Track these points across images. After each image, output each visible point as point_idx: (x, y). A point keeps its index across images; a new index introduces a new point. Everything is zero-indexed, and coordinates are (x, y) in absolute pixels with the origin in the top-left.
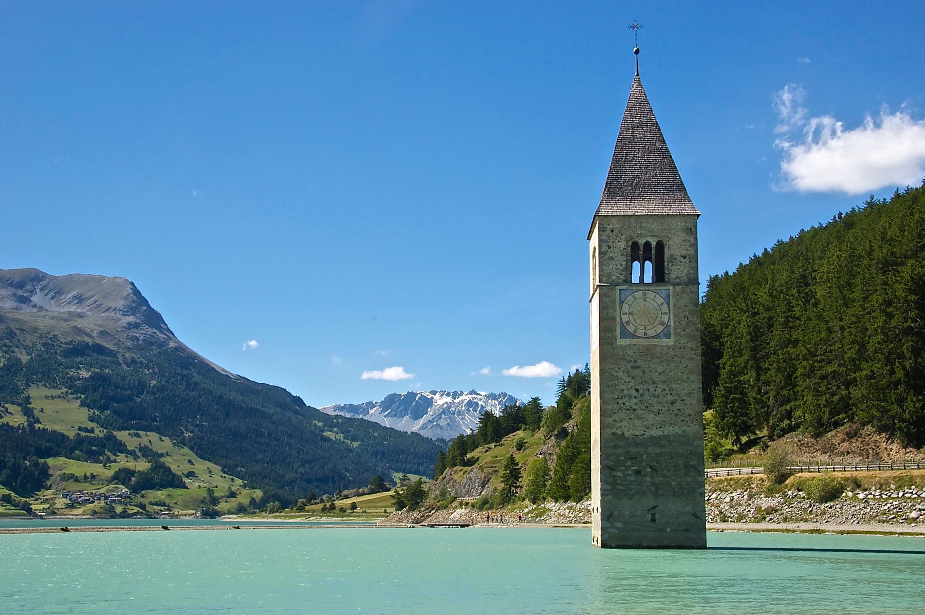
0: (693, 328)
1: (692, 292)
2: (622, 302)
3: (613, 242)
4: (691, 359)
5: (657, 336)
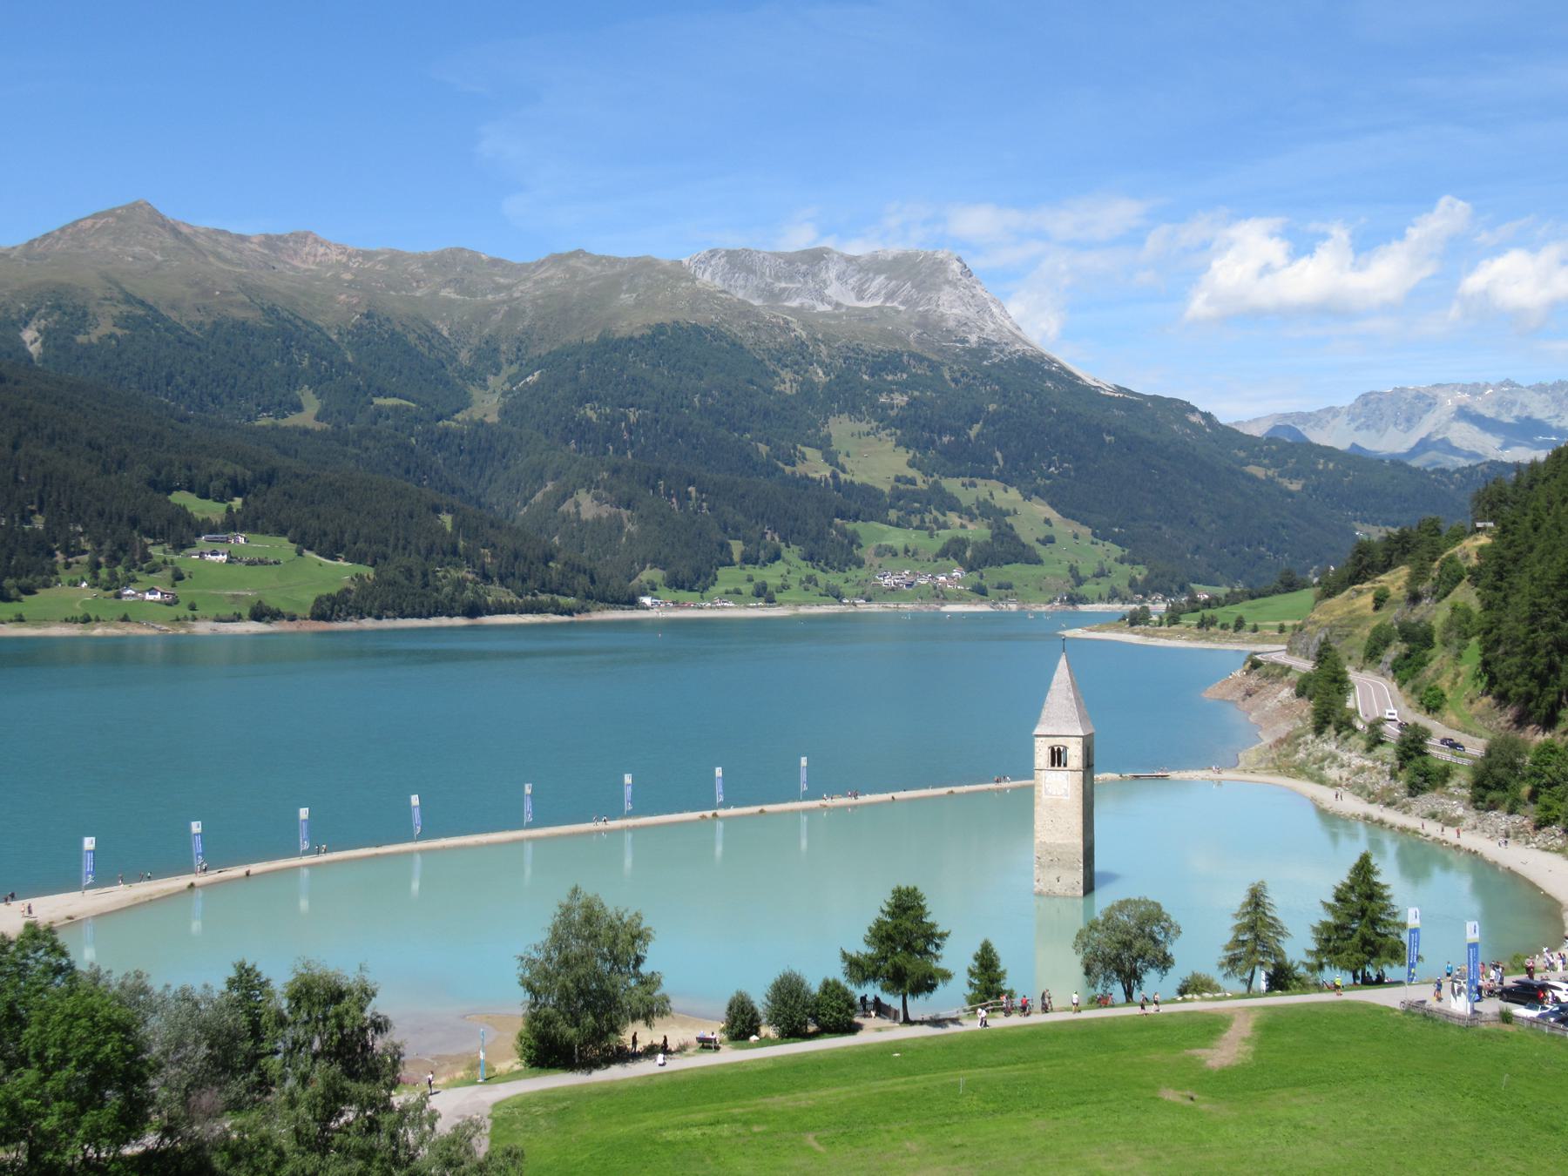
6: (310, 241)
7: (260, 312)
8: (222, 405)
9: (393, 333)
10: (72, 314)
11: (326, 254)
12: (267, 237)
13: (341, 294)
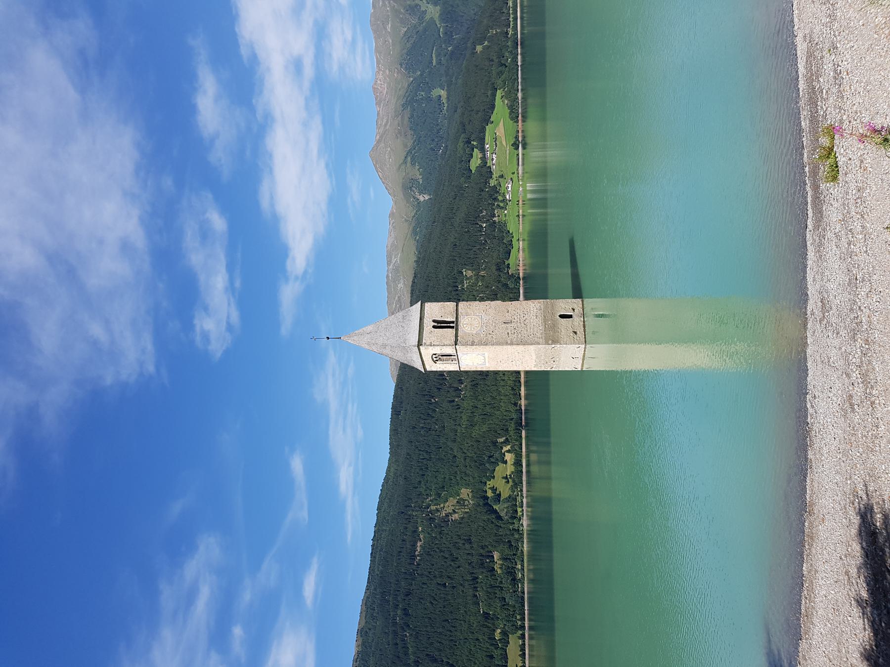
4: (495, 348)
6: (376, 87)
7: (404, 111)
8: (441, 129)
9: (407, 54)
10: (413, 184)
11: (380, 80)
12: (376, 104)
13: (394, 76)
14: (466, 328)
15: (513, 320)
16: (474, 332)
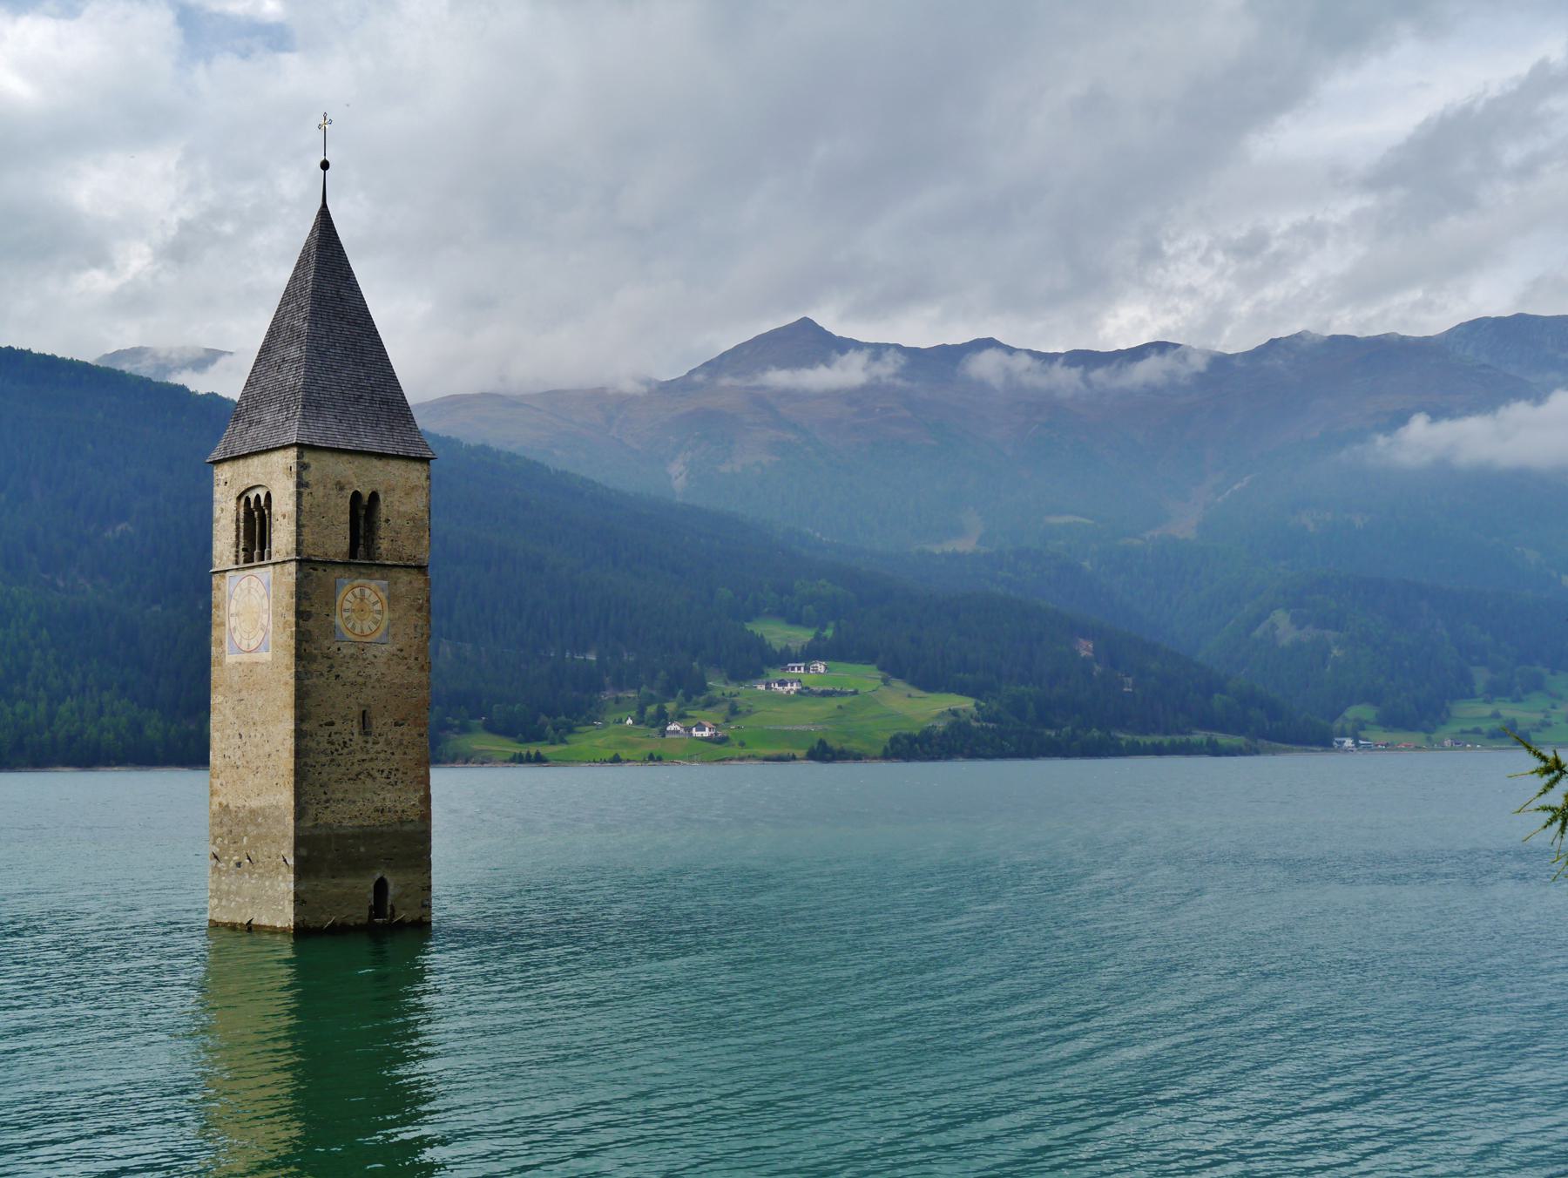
0: (288, 632)
1: (290, 574)
2: (231, 596)
3: (226, 502)
4: (286, 683)
5: (256, 650)
14: (350, 595)
15: (370, 739)
16: (338, 621)
